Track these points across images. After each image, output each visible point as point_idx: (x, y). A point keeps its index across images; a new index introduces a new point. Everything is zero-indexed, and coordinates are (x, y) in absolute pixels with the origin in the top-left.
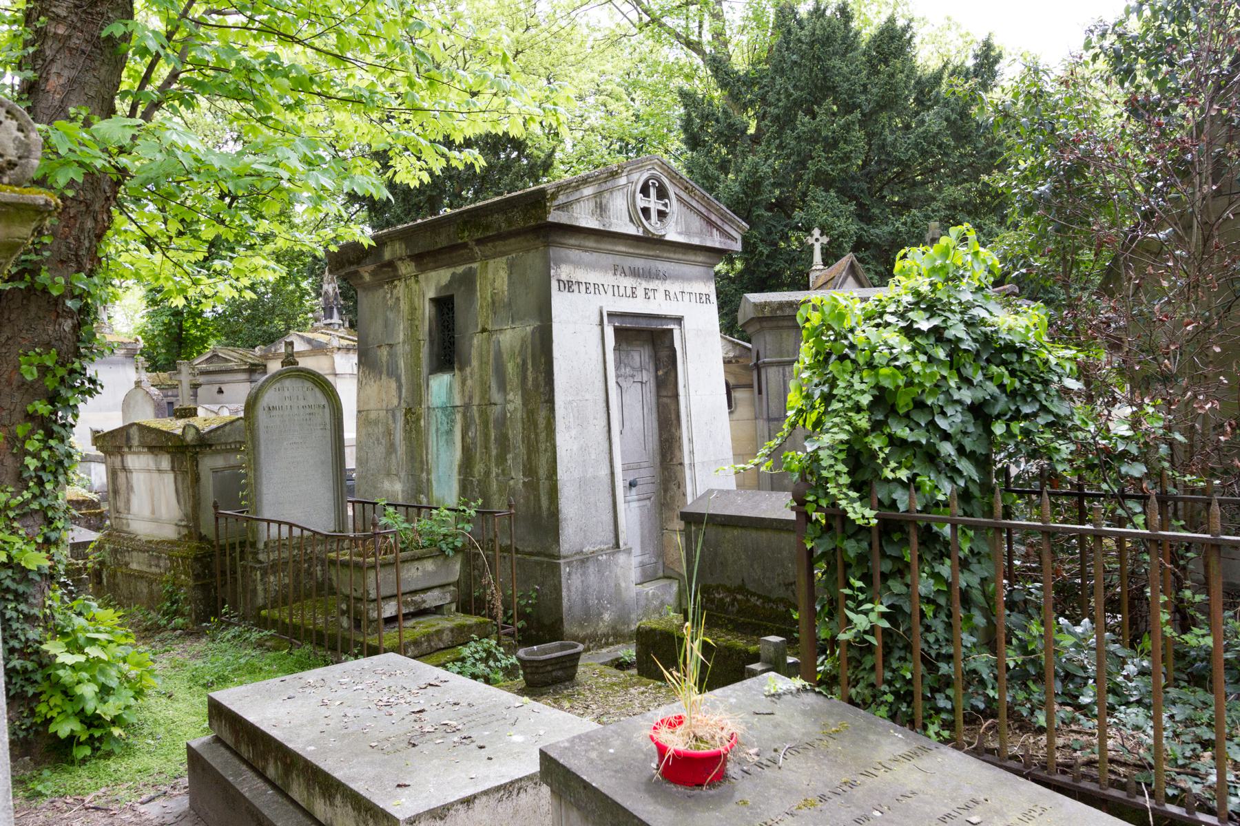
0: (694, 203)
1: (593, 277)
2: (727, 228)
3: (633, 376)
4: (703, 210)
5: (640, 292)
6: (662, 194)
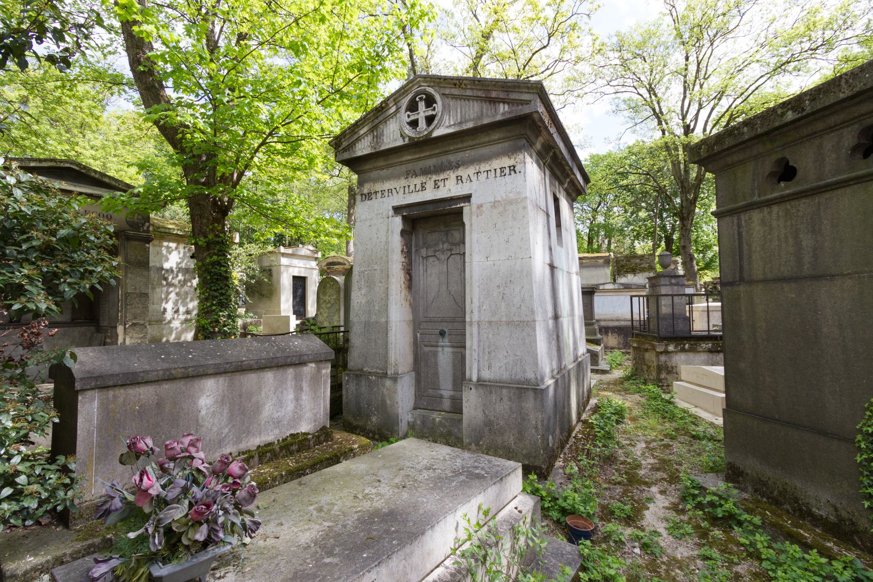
0: (469, 93)
1: (387, 185)
2: (513, 96)
3: (451, 250)
4: (480, 94)
5: (430, 185)
6: (430, 102)
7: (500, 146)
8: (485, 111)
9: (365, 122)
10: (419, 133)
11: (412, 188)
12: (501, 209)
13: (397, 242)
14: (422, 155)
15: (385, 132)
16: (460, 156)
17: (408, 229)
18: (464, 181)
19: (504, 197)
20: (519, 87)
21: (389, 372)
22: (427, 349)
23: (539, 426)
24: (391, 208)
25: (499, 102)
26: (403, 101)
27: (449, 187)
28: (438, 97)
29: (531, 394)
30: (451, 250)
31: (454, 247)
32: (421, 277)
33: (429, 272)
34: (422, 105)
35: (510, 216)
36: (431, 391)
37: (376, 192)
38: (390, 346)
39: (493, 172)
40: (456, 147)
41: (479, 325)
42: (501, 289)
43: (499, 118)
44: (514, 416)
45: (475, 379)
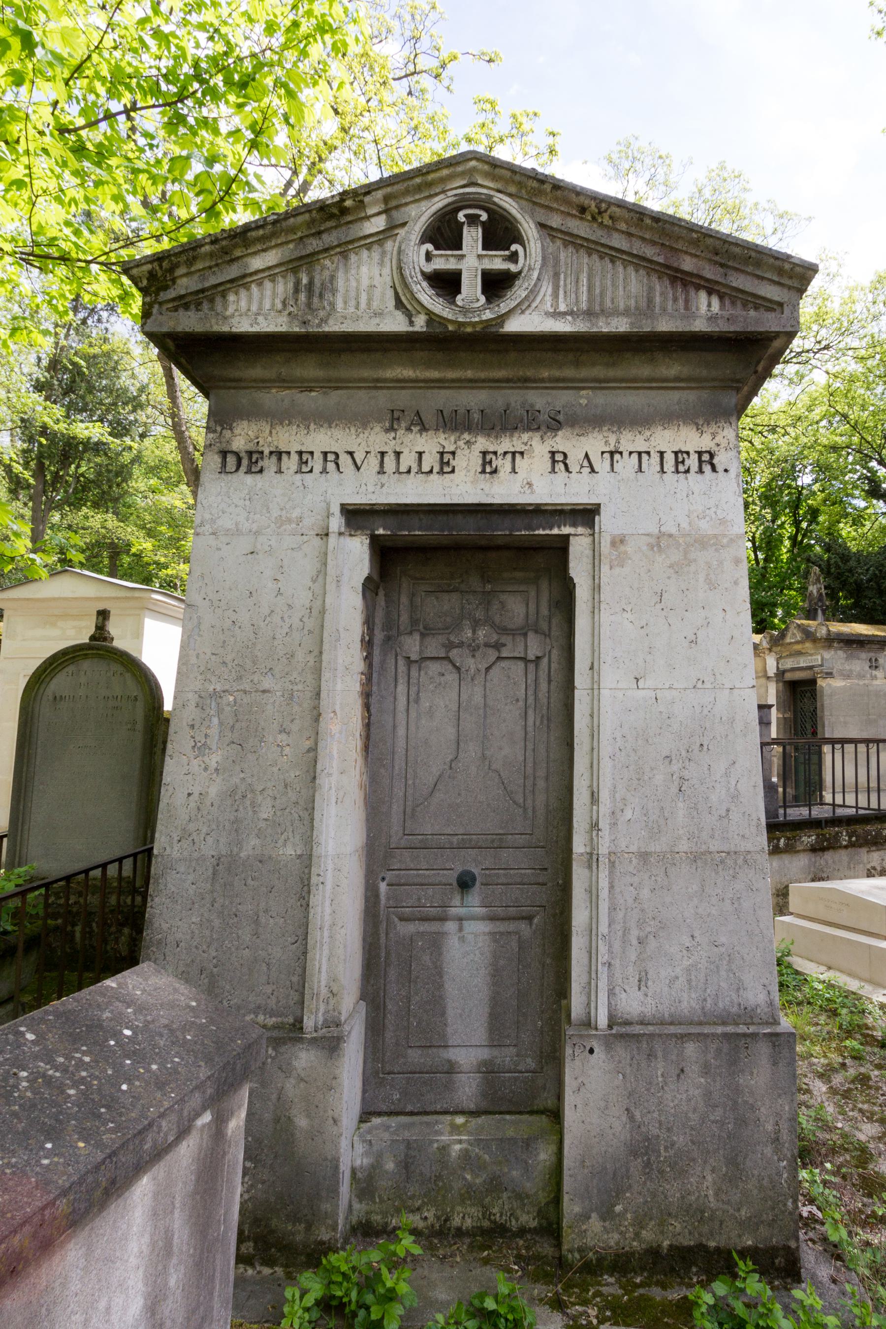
0: (618, 241)
1: (320, 440)
2: (739, 281)
3: (498, 646)
4: (649, 252)
5: (467, 460)
6: (500, 233)
7: (675, 395)
8: (658, 299)
9: (274, 235)
10: (464, 310)
11: (408, 460)
12: (675, 556)
13: (348, 609)
14: (451, 374)
15: (340, 283)
16: (562, 399)
17: (376, 577)
18: (574, 467)
19: (685, 525)
20: (758, 264)
21: (309, 1023)
22: (407, 929)
23: (785, 1136)
24: (336, 510)
25: (698, 287)
26: (412, 211)
27: (528, 477)
28: (528, 228)
29: (763, 1049)
30: (498, 646)
31: (504, 639)
32: (401, 716)
33: (425, 704)
34: (472, 237)
35: (701, 578)
36: (414, 1056)
37: (279, 454)
38: (314, 935)
39: (655, 458)
40: (557, 373)
41: (612, 864)
42: (675, 767)
43: (700, 325)
44: (717, 1114)
45: (602, 1020)
